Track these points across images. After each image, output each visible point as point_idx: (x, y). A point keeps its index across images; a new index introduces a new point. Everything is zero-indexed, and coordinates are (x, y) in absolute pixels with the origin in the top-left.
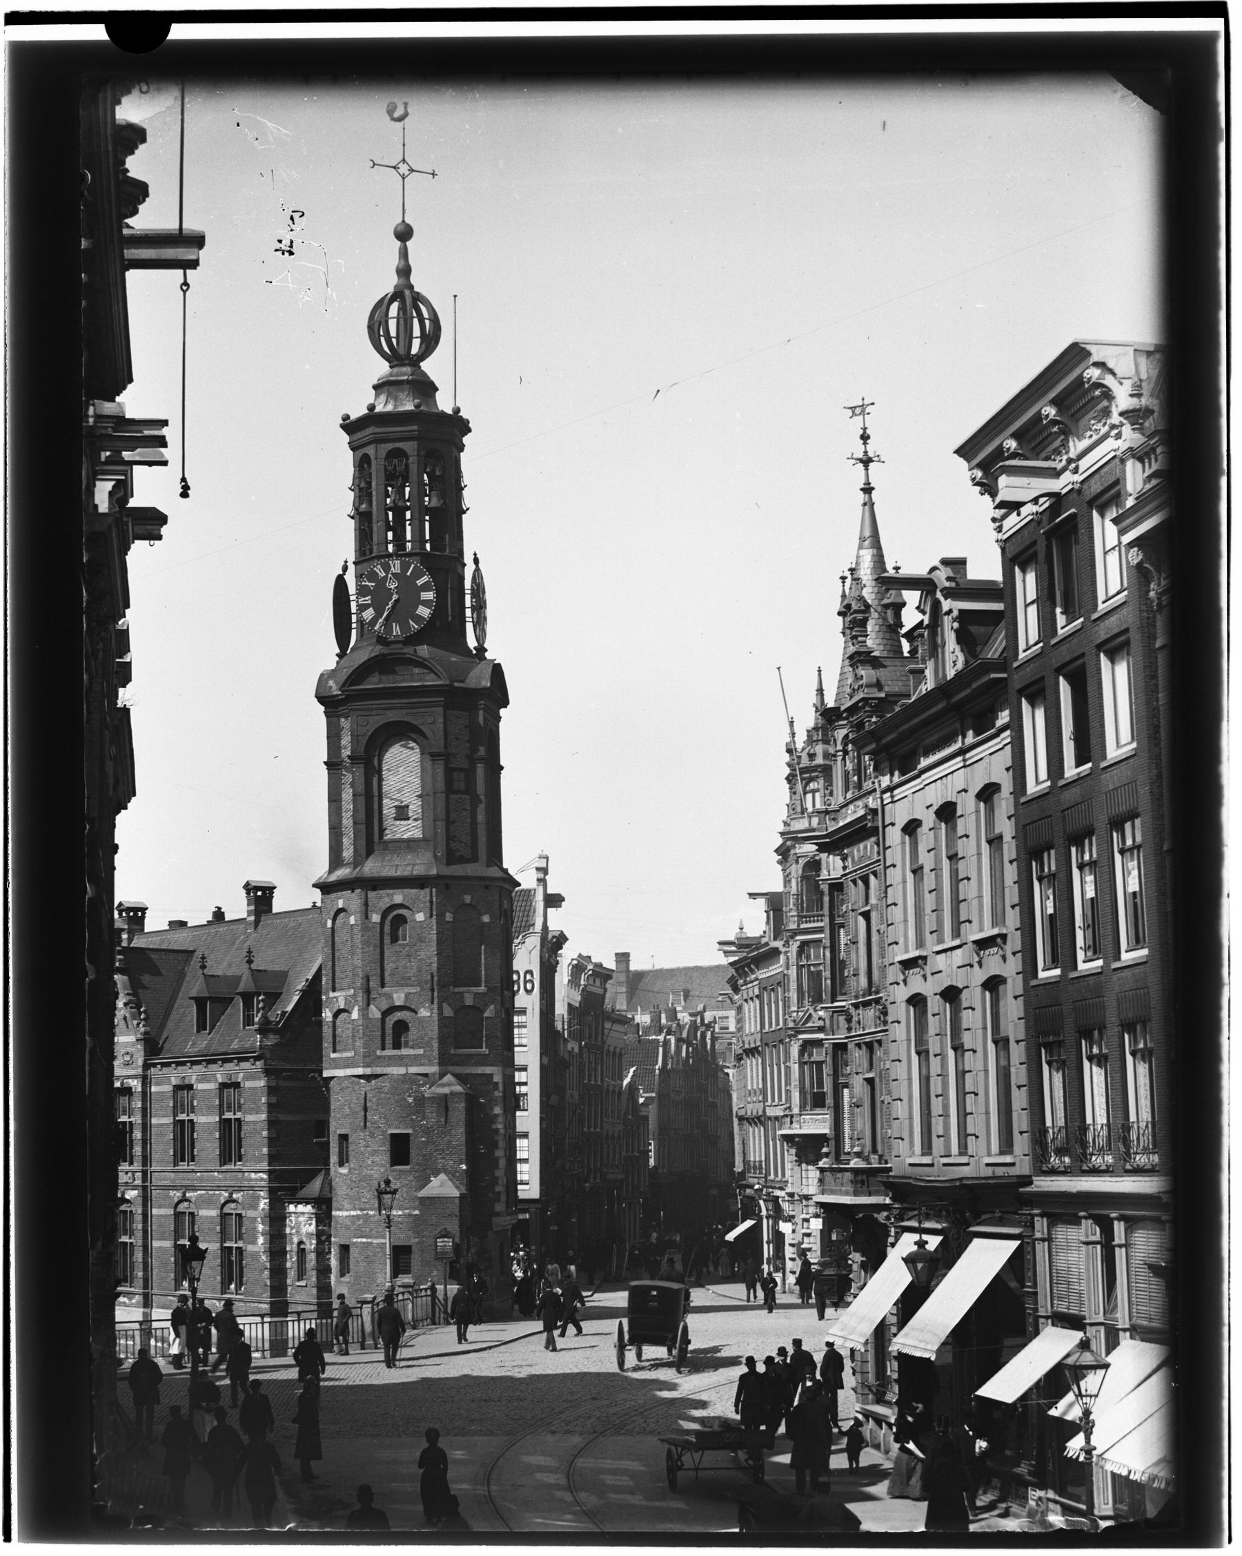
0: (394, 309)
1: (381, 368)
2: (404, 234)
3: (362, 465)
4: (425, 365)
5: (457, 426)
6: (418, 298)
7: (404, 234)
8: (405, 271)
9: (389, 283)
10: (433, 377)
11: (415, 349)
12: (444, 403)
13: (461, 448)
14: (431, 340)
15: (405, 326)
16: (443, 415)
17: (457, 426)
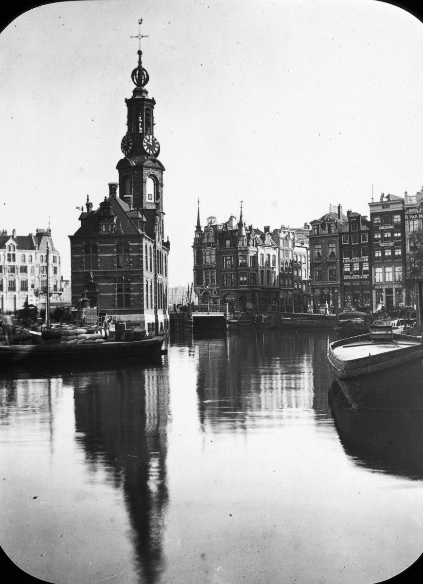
7: (140, 53)
8: (140, 62)
15: (140, 76)
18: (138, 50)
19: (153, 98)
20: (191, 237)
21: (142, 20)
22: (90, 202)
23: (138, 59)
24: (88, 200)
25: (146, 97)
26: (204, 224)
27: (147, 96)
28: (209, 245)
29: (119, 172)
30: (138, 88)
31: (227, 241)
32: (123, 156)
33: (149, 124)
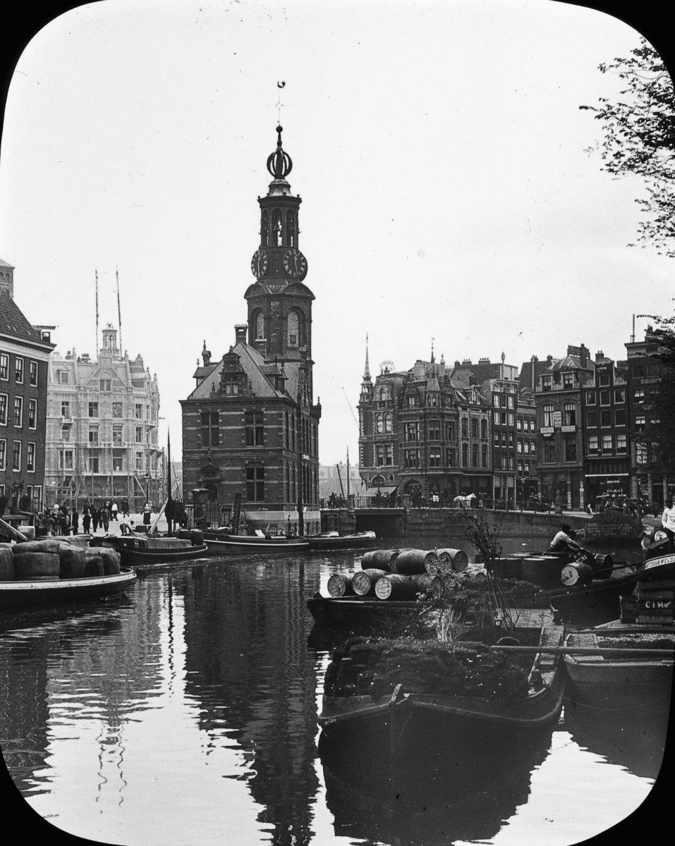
0: (276, 156)
1: (272, 178)
2: (279, 129)
3: (264, 214)
4: (287, 178)
5: (298, 200)
6: (284, 153)
7: (279, 129)
8: (279, 143)
9: (274, 148)
10: (290, 183)
11: (283, 173)
12: (293, 193)
13: (298, 209)
14: (288, 171)
16: (293, 198)
17: (298, 200)
18: (277, 125)
19: (298, 196)
20: (355, 393)
21: (284, 84)
22: (207, 349)
23: (277, 140)
24: (205, 347)
25: (288, 194)
26: (375, 373)
27: (290, 192)
28: (382, 403)
29: (248, 303)
30: (277, 180)
31: (410, 399)
32: (254, 280)
33: (292, 231)
